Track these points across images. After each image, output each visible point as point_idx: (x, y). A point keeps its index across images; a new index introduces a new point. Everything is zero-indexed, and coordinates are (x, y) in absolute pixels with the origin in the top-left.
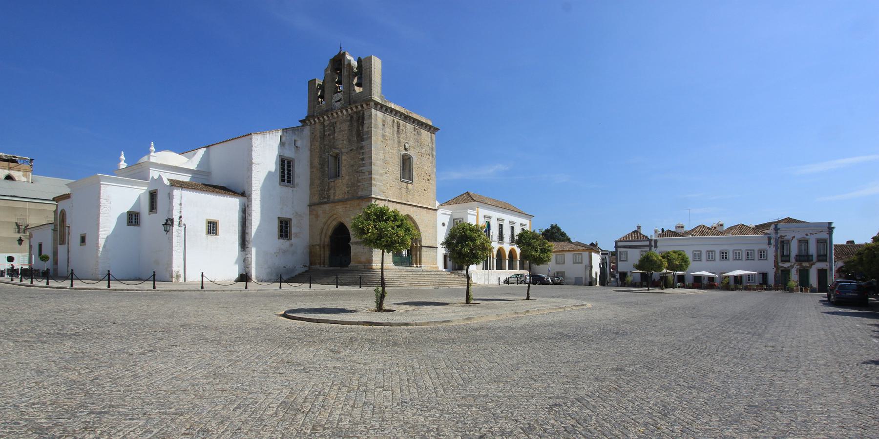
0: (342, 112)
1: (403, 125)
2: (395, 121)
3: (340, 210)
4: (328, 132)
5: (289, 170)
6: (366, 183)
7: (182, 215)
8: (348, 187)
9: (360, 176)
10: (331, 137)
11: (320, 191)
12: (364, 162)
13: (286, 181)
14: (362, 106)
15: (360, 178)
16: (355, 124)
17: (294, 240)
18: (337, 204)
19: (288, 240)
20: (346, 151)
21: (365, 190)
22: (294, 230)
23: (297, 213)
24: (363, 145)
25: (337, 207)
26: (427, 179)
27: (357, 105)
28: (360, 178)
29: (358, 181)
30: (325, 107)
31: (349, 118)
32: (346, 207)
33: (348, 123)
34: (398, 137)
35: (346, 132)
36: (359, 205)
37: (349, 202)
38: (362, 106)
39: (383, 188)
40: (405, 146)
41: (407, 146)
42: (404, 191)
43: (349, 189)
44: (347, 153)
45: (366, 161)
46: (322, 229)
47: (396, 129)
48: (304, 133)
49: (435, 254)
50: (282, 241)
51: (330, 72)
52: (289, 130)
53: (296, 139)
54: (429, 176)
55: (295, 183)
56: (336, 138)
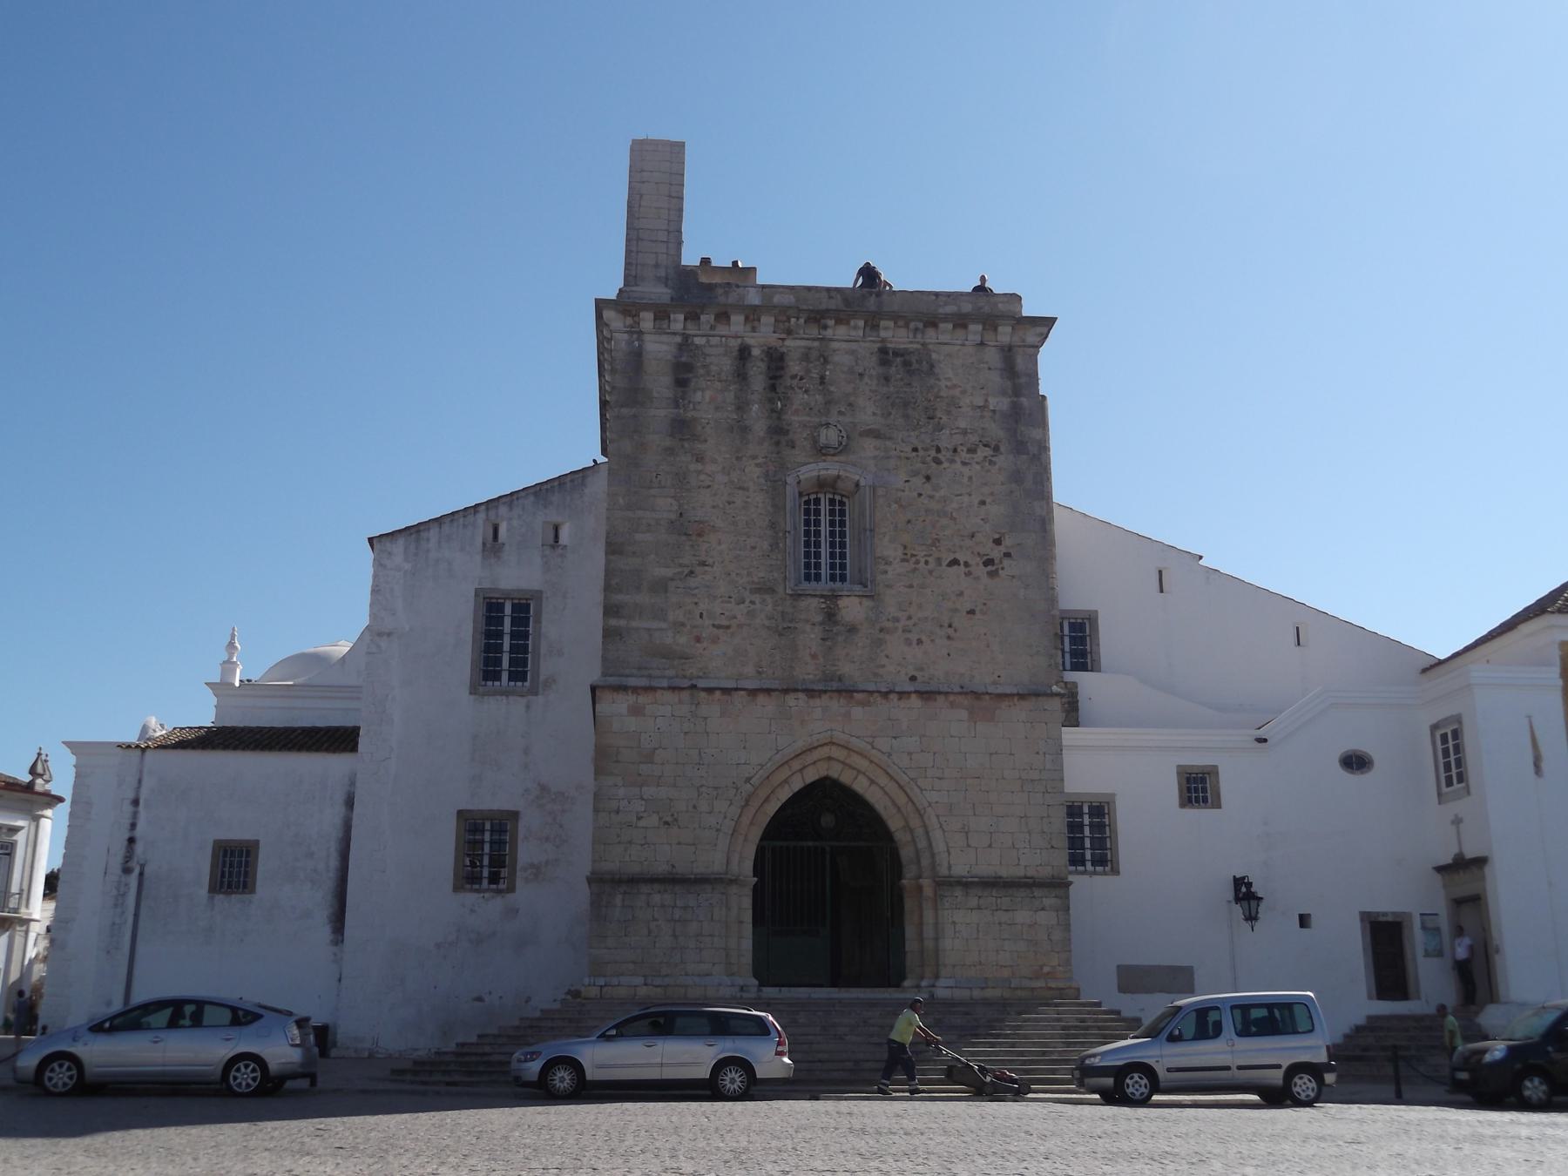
1: (806, 357)
2: (756, 352)
5: (520, 635)
7: (138, 832)
13: (505, 676)
17: (524, 893)
19: (499, 892)
22: (527, 852)
23: (544, 788)
26: (975, 562)
34: (773, 411)
39: (669, 641)
40: (815, 441)
41: (829, 436)
42: (810, 638)
47: (758, 381)
48: (586, 491)
49: (1046, 918)
50: (470, 898)
52: (523, 494)
53: (556, 519)
54: (998, 542)
55: (542, 678)
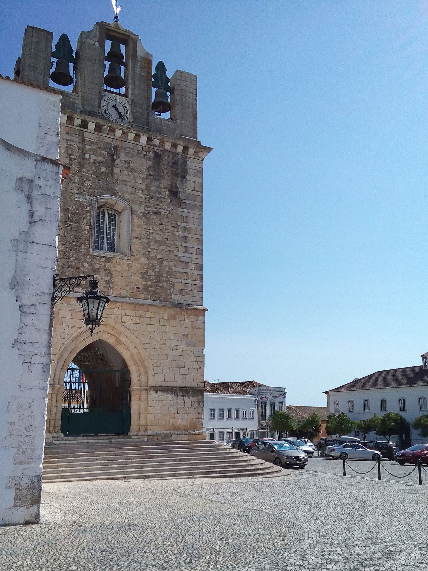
0: (137, 136)
3: (126, 319)
4: (93, 157)
6: (190, 282)
8: (143, 278)
9: (175, 266)
10: (103, 169)
11: (63, 268)
12: (184, 244)
14: (186, 149)
15: (176, 269)
16: (165, 171)
18: (118, 305)
20: (143, 211)
21: (188, 294)
24: (184, 214)
25: (117, 312)
27: (178, 142)
28: (176, 269)
29: (171, 273)
30: (80, 102)
31: (151, 154)
32: (141, 316)
33: (150, 164)
35: (144, 176)
36: (174, 317)
37: (152, 309)
38: (186, 149)
43: (149, 283)
44: (144, 215)
45: (192, 244)
46: (65, 349)
51: (97, 44)
56: (116, 177)
